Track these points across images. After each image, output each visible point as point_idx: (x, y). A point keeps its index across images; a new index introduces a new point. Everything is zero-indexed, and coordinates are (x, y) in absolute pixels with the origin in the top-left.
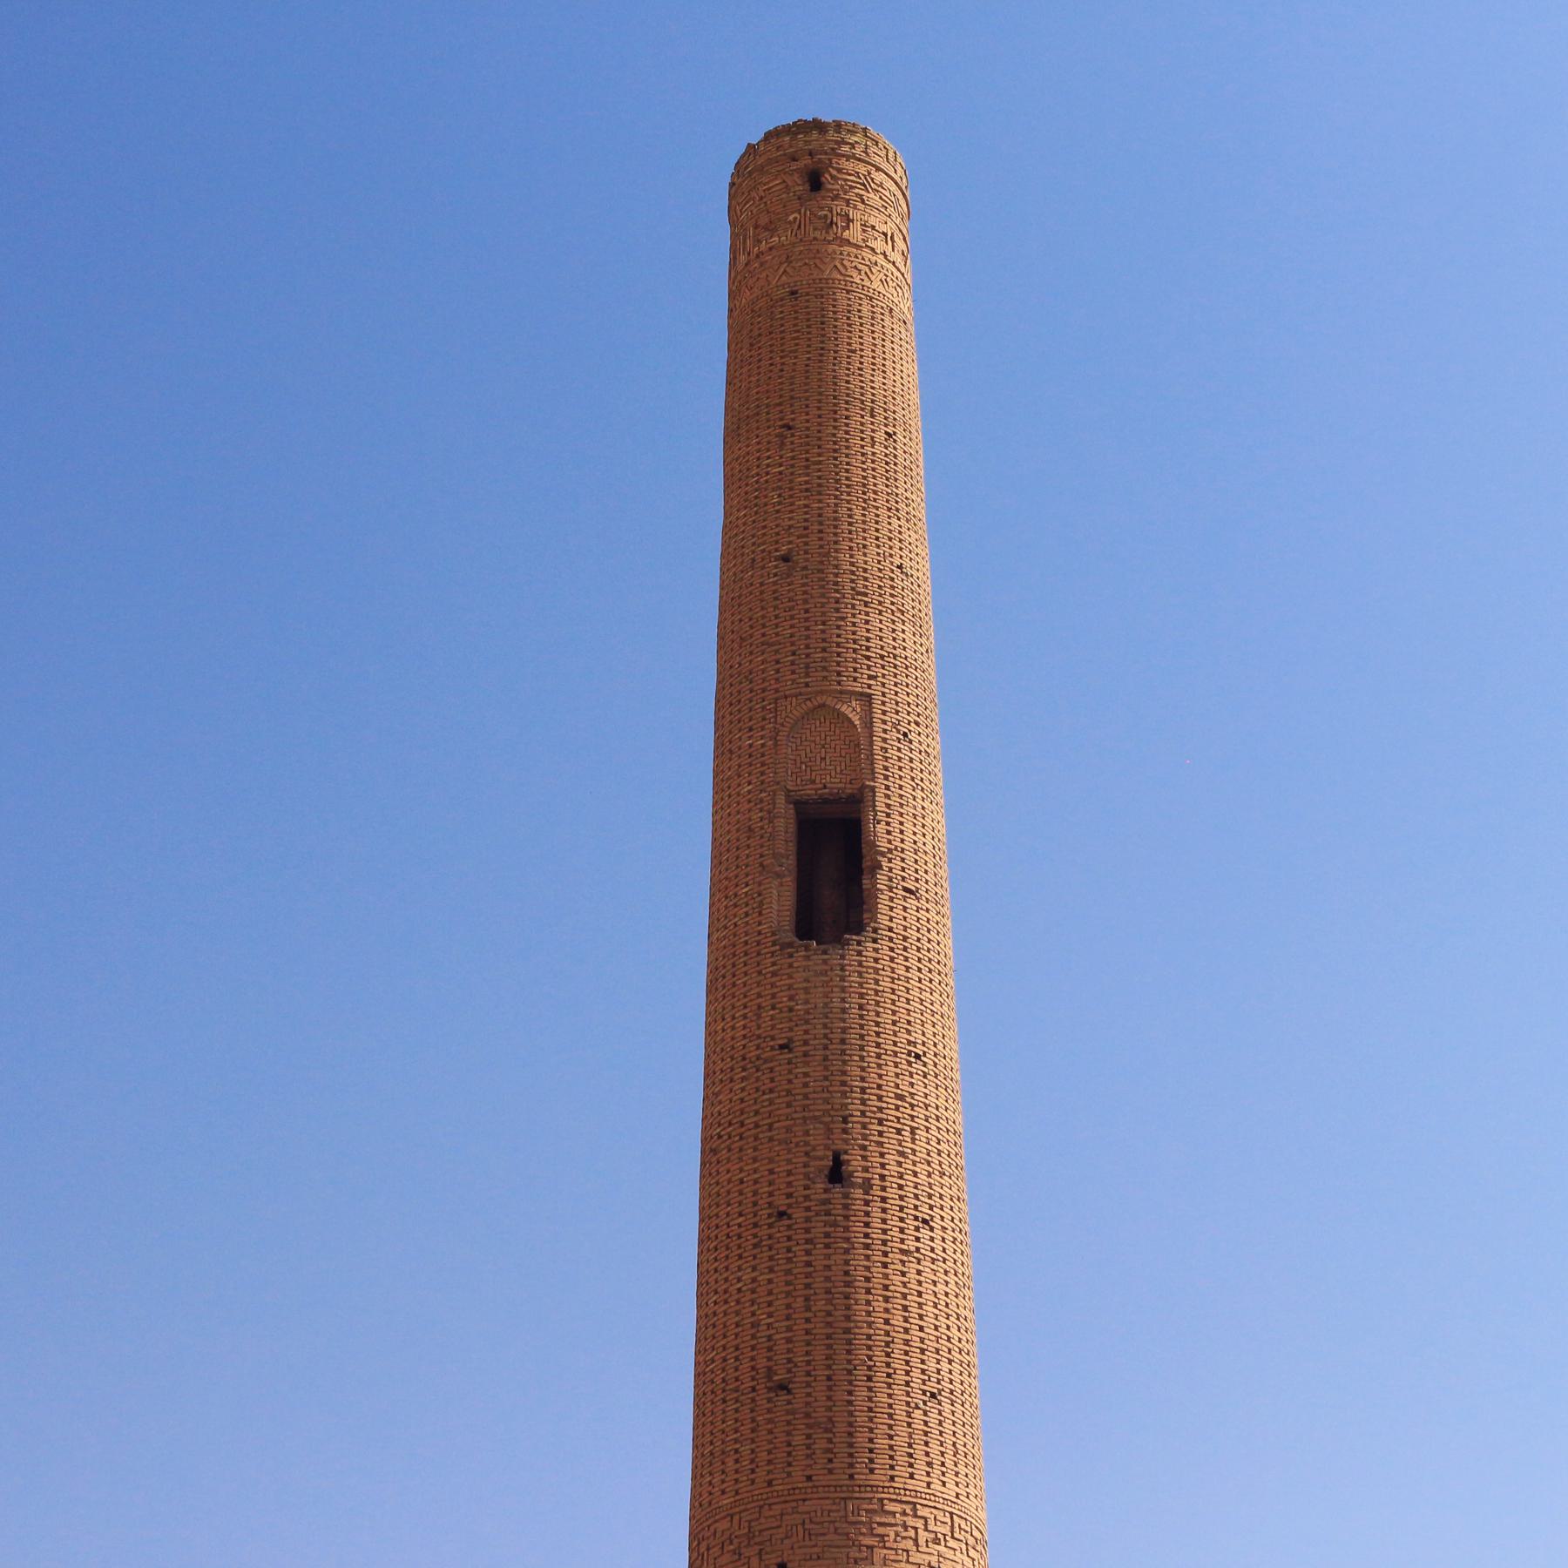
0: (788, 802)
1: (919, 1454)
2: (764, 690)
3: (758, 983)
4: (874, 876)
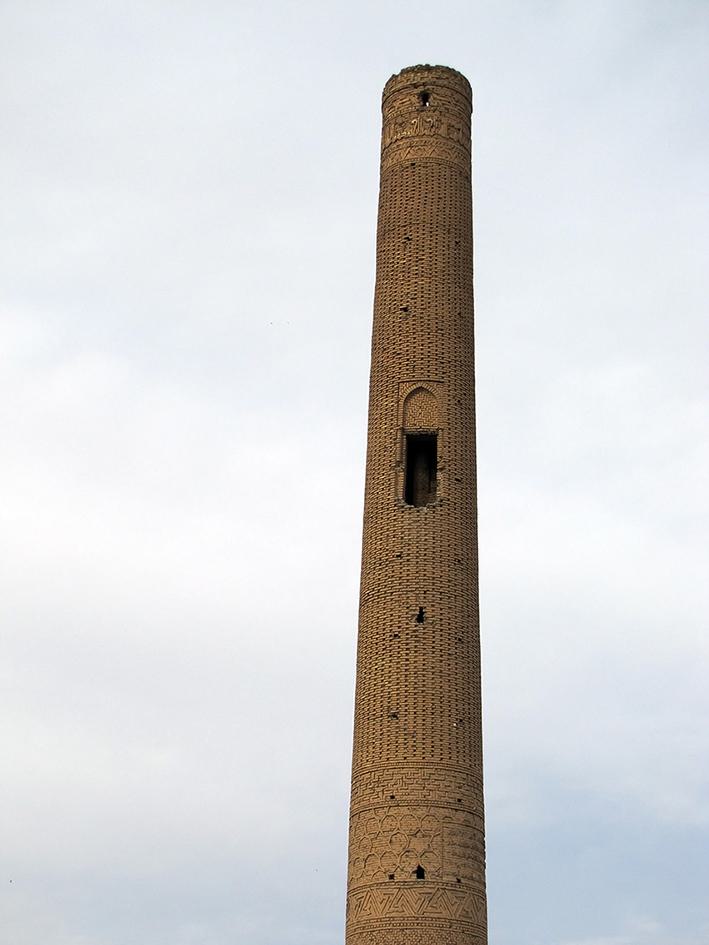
0: (403, 435)
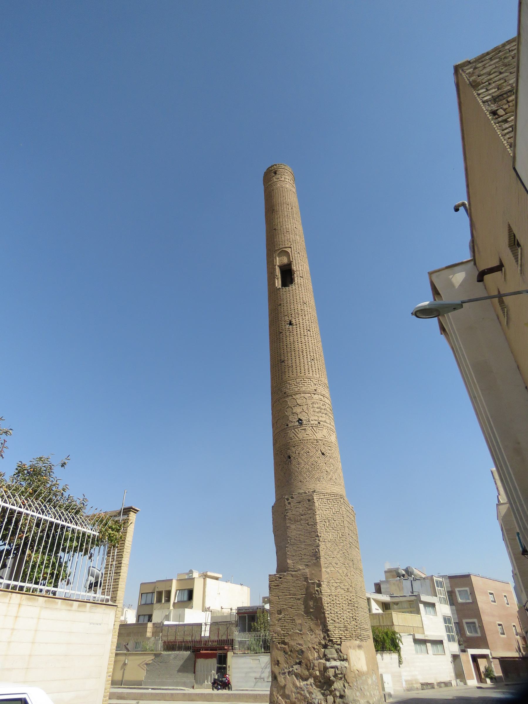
1: (310, 369)
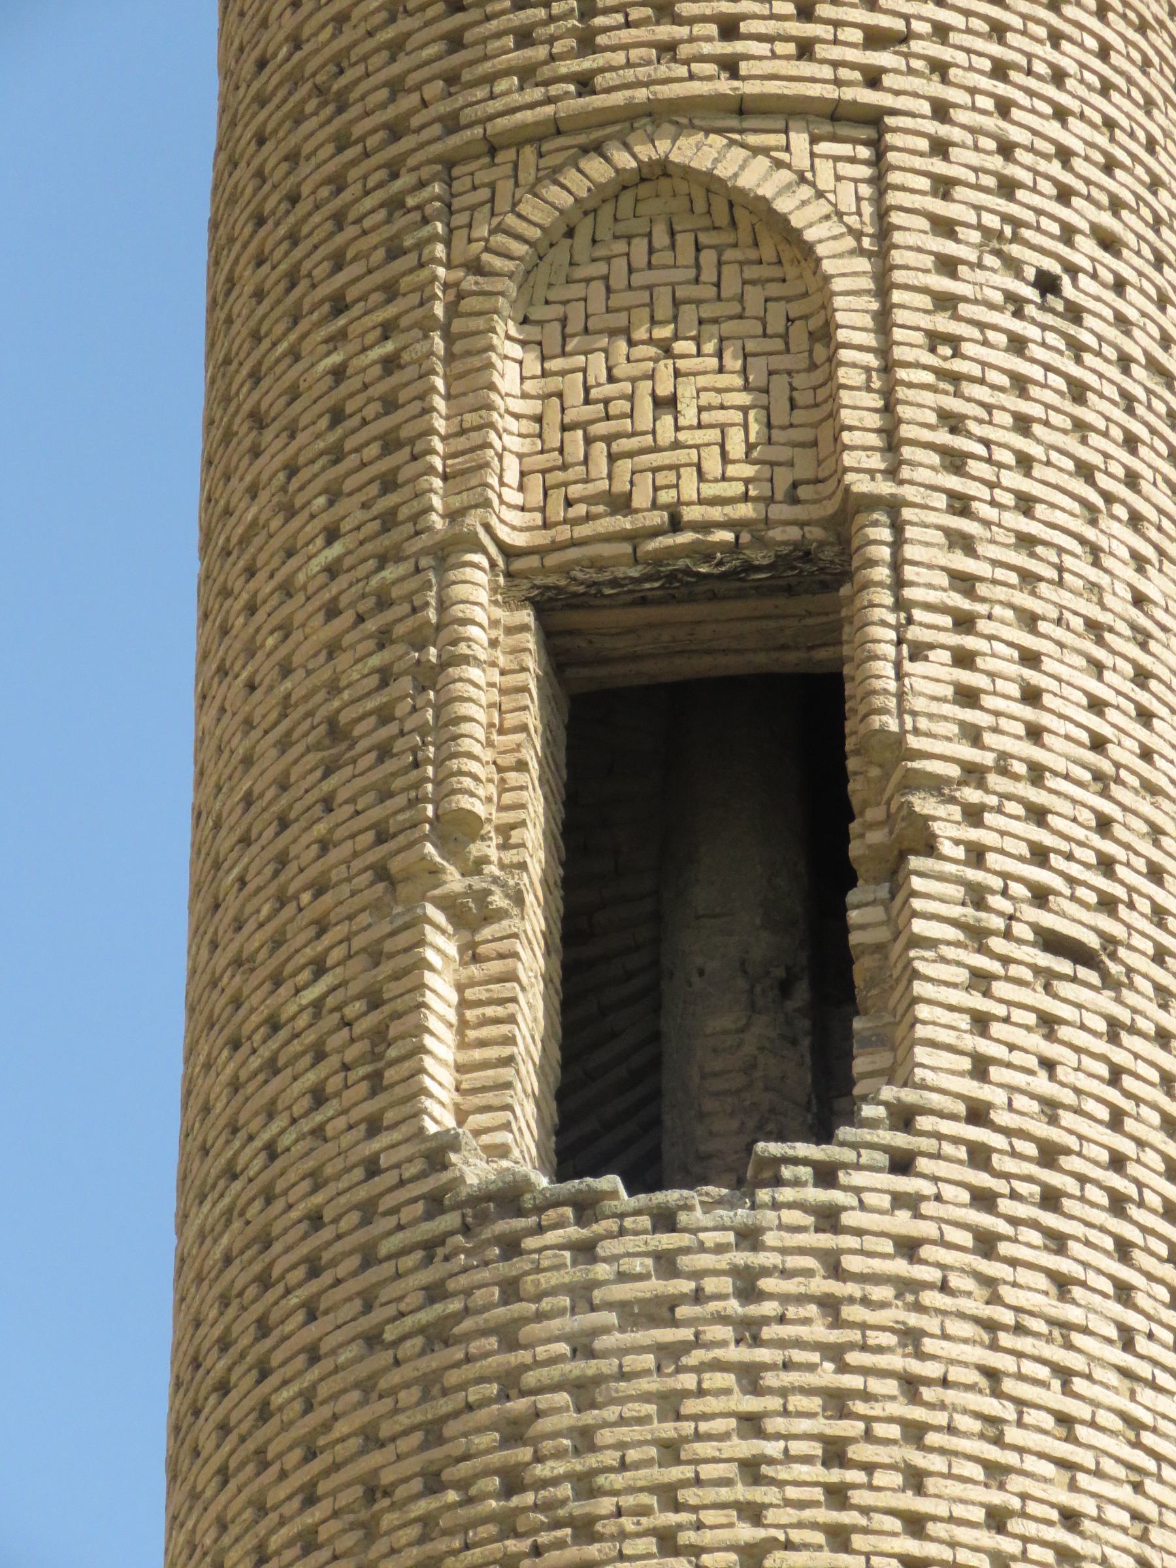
2: (395, 131)
3: (367, 1386)
4: (894, 874)
